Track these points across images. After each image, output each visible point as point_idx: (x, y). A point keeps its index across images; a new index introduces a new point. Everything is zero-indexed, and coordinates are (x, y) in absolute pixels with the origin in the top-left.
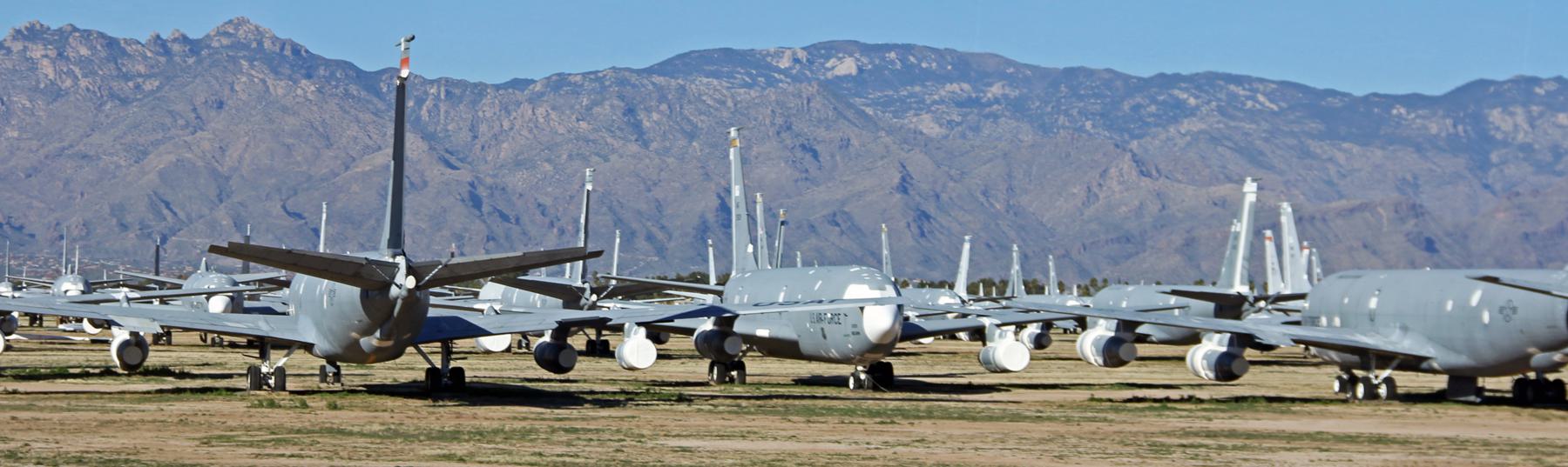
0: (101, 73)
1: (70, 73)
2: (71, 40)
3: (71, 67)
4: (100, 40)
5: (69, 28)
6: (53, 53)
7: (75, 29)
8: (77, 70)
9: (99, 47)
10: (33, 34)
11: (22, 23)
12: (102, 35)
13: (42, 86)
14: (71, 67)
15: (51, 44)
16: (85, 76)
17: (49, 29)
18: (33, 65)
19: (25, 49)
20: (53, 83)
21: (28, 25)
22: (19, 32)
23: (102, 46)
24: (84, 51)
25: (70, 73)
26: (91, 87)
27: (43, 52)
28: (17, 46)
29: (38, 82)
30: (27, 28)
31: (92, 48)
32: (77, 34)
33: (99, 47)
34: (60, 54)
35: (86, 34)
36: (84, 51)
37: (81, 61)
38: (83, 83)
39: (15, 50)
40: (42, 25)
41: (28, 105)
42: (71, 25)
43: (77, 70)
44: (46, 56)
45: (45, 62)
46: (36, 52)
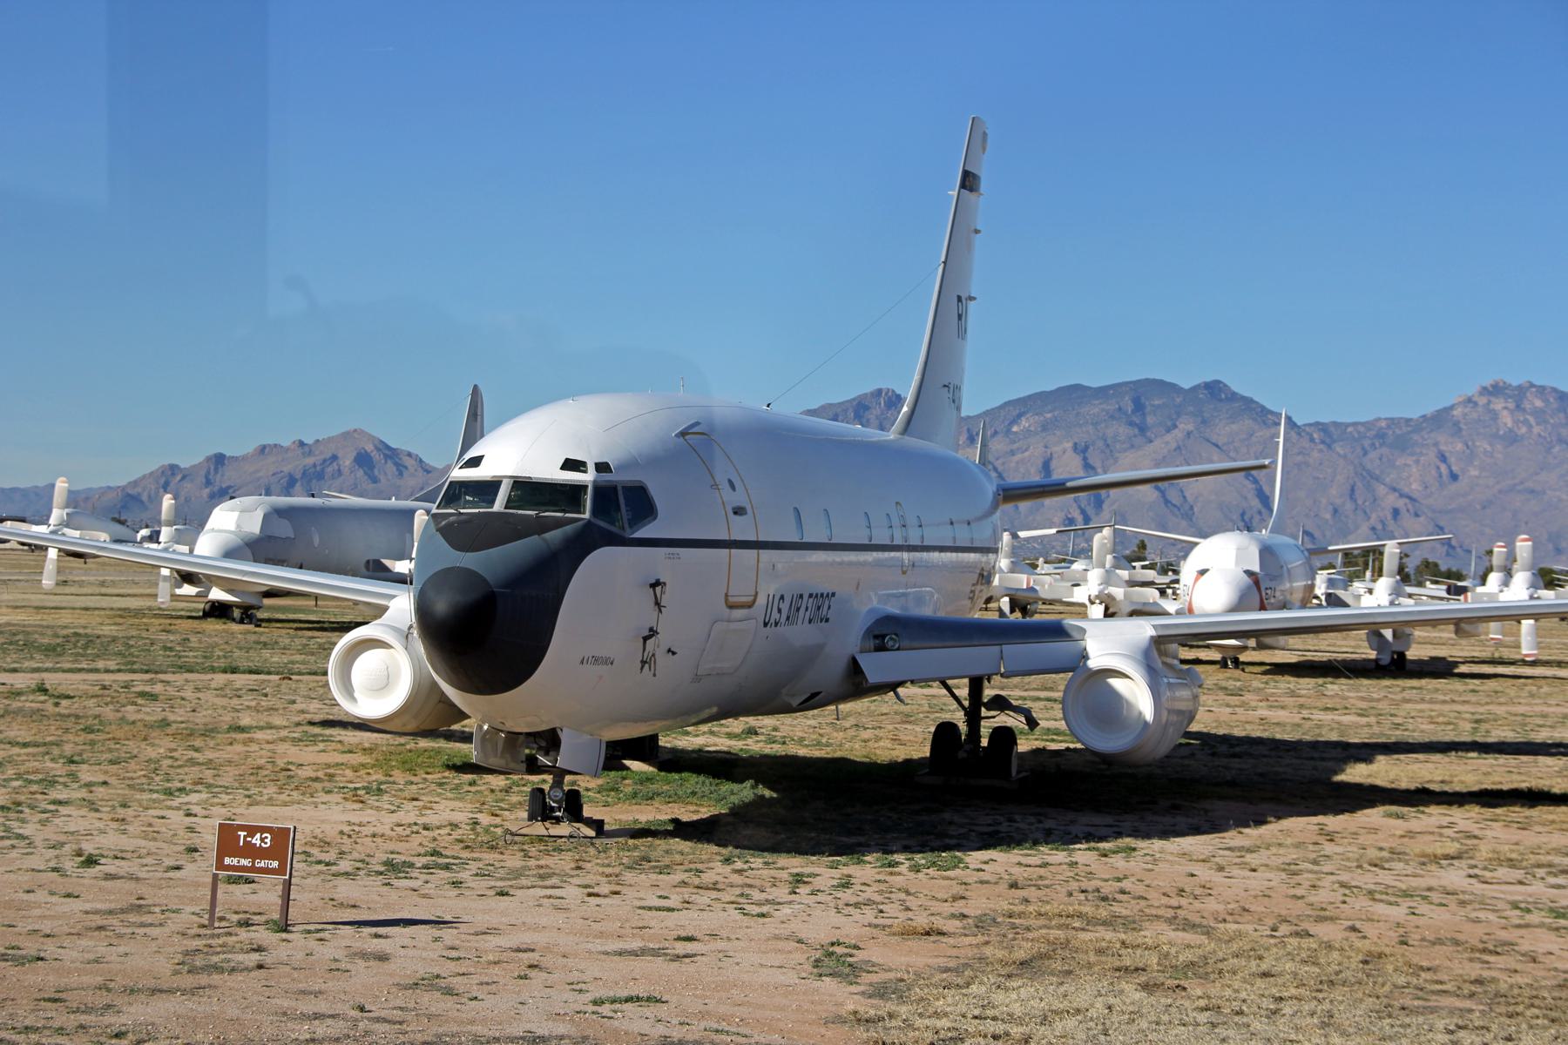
0: (1552, 421)
1: (1526, 422)
2: (1528, 394)
3: (1528, 417)
4: (1554, 394)
5: (1528, 385)
6: (1511, 405)
7: (1532, 385)
8: (1532, 420)
9: (1552, 400)
10: (1496, 390)
11: (1487, 382)
12: (1554, 390)
13: (1501, 432)
14: (1528, 417)
15: (1510, 397)
16: (1538, 424)
17: (1510, 385)
18: (1495, 416)
19: (1489, 402)
20: (1511, 430)
21: (1493, 383)
22: (1485, 388)
23: (1555, 399)
24: (1539, 403)
25: (1526, 422)
26: (1542, 434)
27: (1503, 405)
28: (1482, 401)
29: (1498, 430)
30: (1492, 386)
31: (1546, 401)
32: (1534, 390)
33: (1552, 400)
34: (1518, 406)
35: (1541, 390)
36: (1539, 403)
37: (1537, 413)
38: (1536, 430)
39: (1481, 403)
40: (1505, 383)
41: (1489, 448)
42: (1530, 382)
43: (1532, 420)
44: (1506, 408)
45: (1505, 413)
46: (1498, 404)
